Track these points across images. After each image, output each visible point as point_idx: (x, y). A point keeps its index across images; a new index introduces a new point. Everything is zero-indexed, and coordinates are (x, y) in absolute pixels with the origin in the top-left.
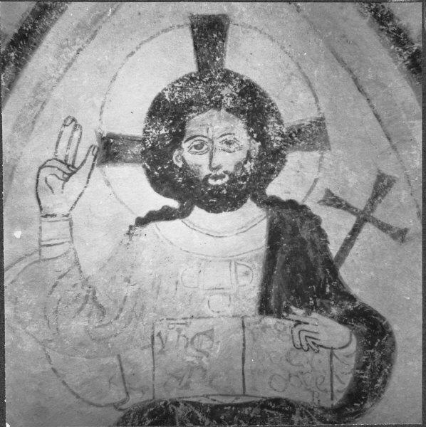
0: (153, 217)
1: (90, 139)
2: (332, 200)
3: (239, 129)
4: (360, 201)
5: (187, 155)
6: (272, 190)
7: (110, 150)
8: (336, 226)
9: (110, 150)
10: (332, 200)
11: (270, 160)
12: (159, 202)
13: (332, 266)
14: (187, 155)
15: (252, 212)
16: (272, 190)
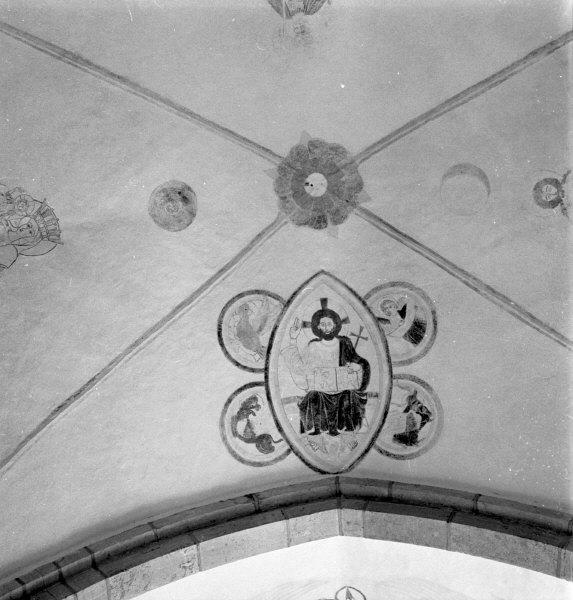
0: (314, 340)
1: (301, 322)
2: (353, 334)
3: (331, 321)
4: (358, 333)
5: (320, 327)
6: (339, 334)
7: (305, 325)
8: (353, 340)
9: (305, 325)
10: (353, 334)
11: (338, 328)
12: (315, 337)
13: (354, 350)
14: (320, 327)
15: (335, 342)
16: (339, 334)
